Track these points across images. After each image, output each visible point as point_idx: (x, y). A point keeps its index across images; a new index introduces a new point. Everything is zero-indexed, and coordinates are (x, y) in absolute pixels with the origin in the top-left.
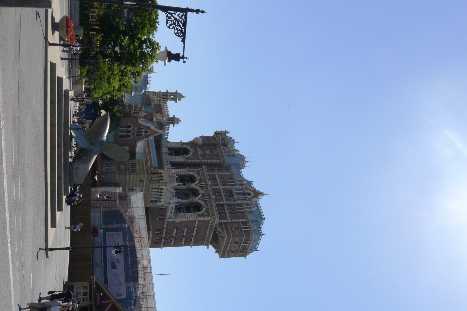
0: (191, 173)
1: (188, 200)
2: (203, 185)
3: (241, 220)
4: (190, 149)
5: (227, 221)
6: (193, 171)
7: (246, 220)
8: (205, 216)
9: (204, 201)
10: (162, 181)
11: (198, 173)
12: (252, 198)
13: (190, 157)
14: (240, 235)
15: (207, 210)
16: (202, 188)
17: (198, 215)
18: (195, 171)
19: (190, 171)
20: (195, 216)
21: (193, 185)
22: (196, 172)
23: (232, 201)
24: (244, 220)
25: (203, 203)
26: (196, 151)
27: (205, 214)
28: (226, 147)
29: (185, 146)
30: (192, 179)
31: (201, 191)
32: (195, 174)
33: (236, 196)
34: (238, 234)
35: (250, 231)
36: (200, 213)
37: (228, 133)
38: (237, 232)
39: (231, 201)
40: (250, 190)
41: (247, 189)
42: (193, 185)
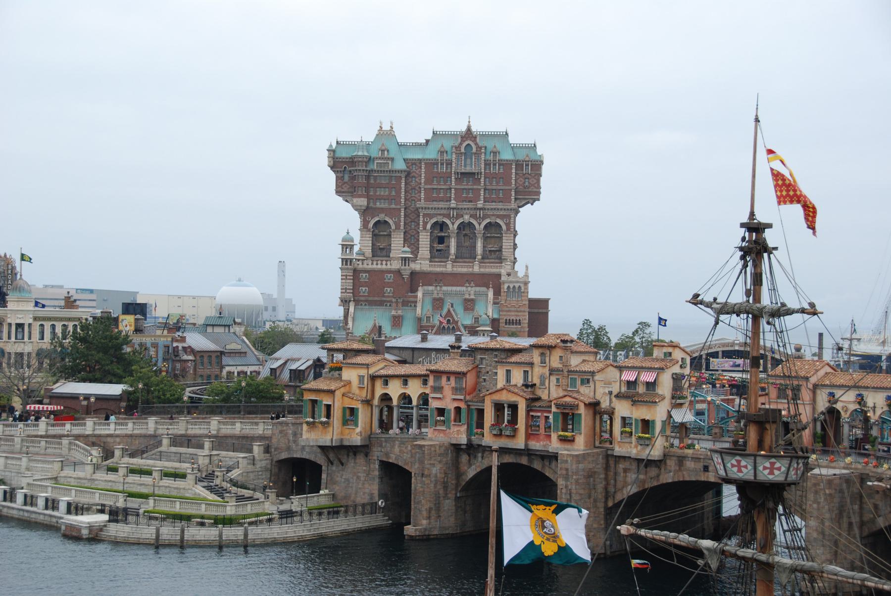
0: (429, 226)
1: (479, 239)
2: (455, 214)
3: (514, 171)
4: (377, 219)
5: (513, 191)
6: (425, 224)
7: (514, 164)
8: (510, 222)
9: (484, 218)
10: (523, 288)
11: (431, 216)
12: (476, 144)
13: (395, 223)
14: (536, 177)
15: (502, 217)
16: (459, 216)
17: (507, 230)
18: (424, 219)
19: (425, 228)
20: (508, 235)
21: (453, 227)
22: (427, 219)
23: (481, 177)
24: (514, 167)
25: (488, 221)
26: (382, 210)
27: (506, 221)
28: (376, 162)
29: (371, 225)
30: (442, 226)
31: (467, 218)
32: (431, 220)
33: (473, 169)
34: (535, 181)
35: (533, 163)
36: (504, 227)
37: (331, 146)
38: (533, 181)
39: (480, 179)
40: (461, 144)
41: (458, 148)
42: (453, 227)
